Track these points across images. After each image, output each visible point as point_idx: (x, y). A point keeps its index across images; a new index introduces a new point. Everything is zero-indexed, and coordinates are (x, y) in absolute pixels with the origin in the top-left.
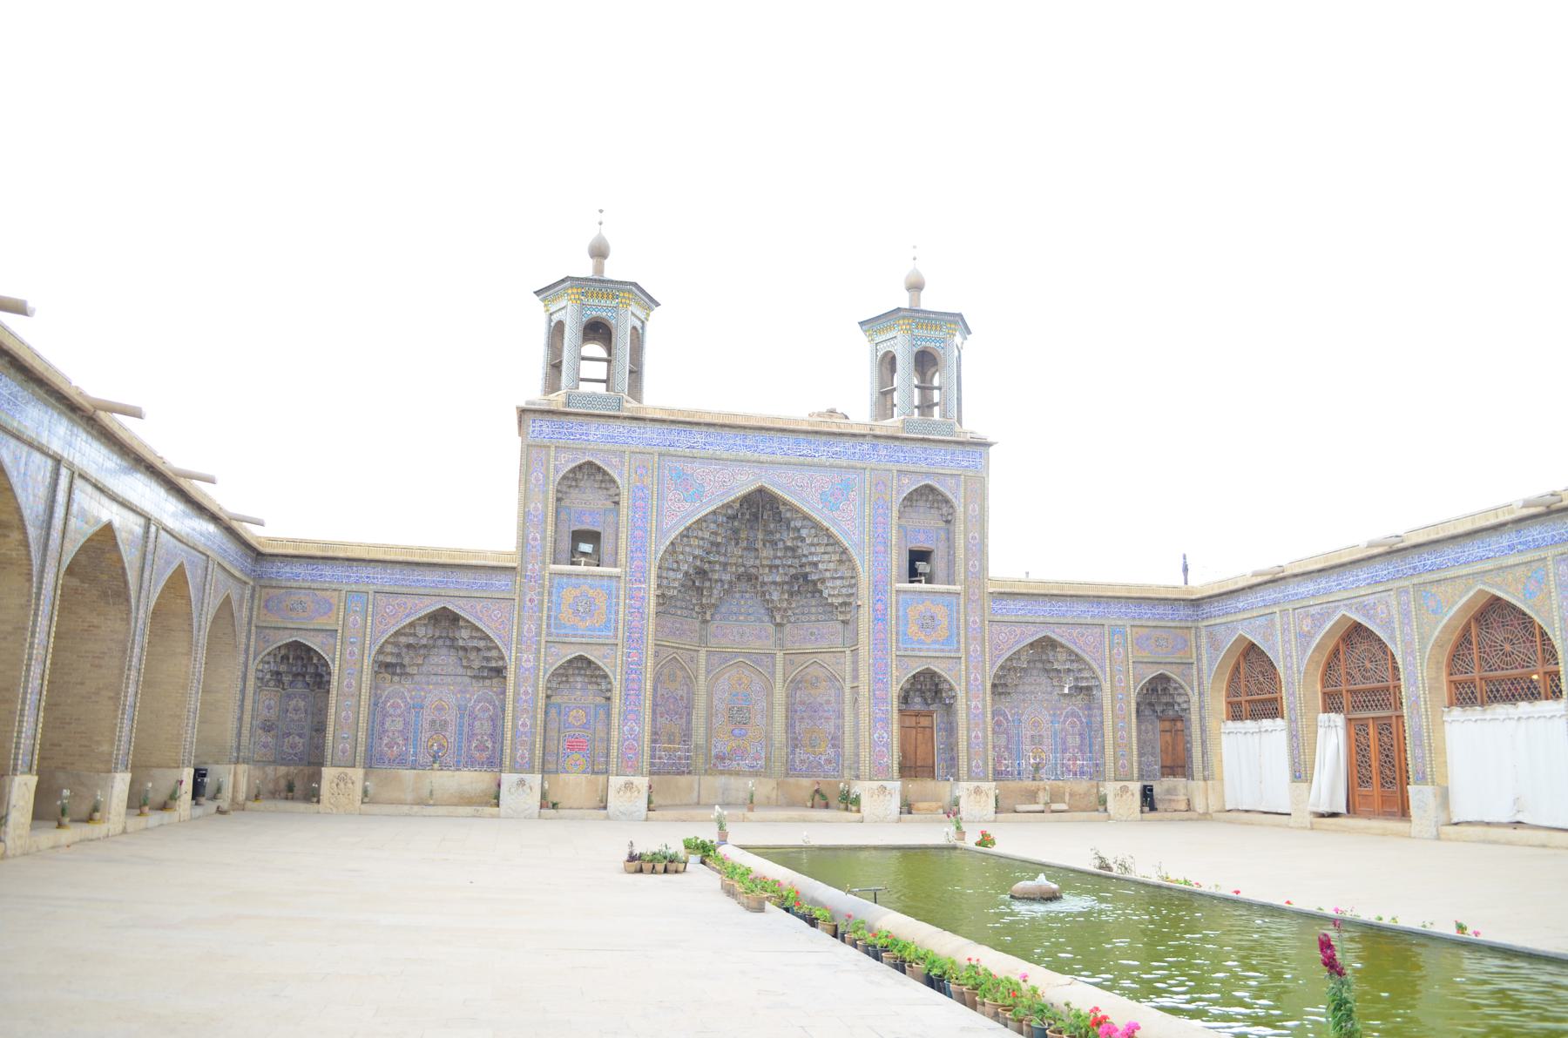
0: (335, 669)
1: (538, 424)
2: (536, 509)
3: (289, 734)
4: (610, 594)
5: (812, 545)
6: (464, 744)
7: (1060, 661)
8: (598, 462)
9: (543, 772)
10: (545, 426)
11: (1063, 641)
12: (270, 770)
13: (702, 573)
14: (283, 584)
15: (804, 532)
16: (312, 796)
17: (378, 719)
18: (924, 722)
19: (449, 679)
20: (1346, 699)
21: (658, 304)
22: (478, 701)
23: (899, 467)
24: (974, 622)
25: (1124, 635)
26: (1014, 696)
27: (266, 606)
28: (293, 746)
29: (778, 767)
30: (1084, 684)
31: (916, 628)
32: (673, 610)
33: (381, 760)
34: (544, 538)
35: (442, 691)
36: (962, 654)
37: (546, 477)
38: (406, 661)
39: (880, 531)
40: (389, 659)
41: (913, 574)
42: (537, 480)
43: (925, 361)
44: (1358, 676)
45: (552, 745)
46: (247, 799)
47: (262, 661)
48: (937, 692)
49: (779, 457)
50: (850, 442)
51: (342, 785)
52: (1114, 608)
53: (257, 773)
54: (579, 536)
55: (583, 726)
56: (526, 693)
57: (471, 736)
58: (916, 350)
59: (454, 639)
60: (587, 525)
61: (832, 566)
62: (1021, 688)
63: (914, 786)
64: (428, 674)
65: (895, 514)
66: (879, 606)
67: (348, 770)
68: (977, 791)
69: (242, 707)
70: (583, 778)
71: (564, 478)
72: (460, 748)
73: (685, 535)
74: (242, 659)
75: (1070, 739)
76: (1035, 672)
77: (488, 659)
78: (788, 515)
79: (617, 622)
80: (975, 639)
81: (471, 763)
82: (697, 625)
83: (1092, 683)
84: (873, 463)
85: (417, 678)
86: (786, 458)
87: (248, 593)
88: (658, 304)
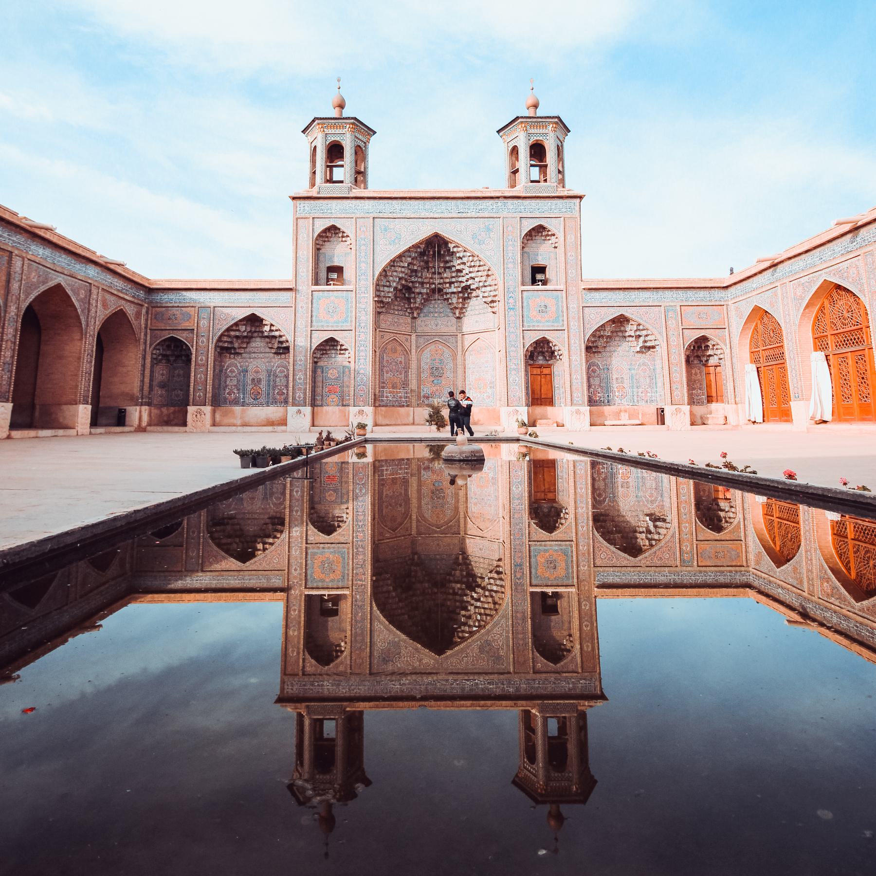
0: (194, 351)
1: (302, 205)
3: (174, 390)
5: (471, 267)
6: (271, 391)
7: (630, 329)
9: (313, 405)
11: (633, 317)
12: (164, 410)
13: (409, 289)
14: (164, 305)
15: (465, 260)
16: (184, 424)
17: (223, 379)
18: (546, 371)
19: (261, 355)
20: (831, 341)
21: (375, 133)
22: (278, 367)
25: (675, 311)
26: (604, 354)
27: (155, 318)
30: (648, 344)
31: (534, 313)
32: (392, 311)
33: (225, 402)
34: (308, 271)
35: (257, 361)
36: (565, 327)
37: (308, 236)
38: (236, 345)
40: (226, 345)
41: (534, 281)
43: (537, 151)
44: (839, 324)
45: (319, 390)
46: (149, 424)
47: (154, 349)
48: (553, 352)
49: (446, 215)
52: (668, 293)
53: (155, 411)
54: (331, 269)
55: (337, 379)
56: (301, 360)
57: (275, 387)
58: (532, 141)
59: (262, 332)
60: (336, 263)
61: (484, 279)
62: (608, 349)
63: (539, 410)
64: (250, 353)
65: (519, 244)
69: (143, 375)
70: (336, 409)
71: (319, 236)
72: (269, 394)
73: (393, 263)
74: (142, 347)
75: (642, 380)
76: (617, 339)
77: (281, 342)
78: (455, 250)
79: (351, 317)
80: (574, 318)
81: (275, 402)
83: (657, 343)
84: (505, 214)
85: (244, 355)
86: (450, 215)
87: (144, 311)
88: (375, 133)
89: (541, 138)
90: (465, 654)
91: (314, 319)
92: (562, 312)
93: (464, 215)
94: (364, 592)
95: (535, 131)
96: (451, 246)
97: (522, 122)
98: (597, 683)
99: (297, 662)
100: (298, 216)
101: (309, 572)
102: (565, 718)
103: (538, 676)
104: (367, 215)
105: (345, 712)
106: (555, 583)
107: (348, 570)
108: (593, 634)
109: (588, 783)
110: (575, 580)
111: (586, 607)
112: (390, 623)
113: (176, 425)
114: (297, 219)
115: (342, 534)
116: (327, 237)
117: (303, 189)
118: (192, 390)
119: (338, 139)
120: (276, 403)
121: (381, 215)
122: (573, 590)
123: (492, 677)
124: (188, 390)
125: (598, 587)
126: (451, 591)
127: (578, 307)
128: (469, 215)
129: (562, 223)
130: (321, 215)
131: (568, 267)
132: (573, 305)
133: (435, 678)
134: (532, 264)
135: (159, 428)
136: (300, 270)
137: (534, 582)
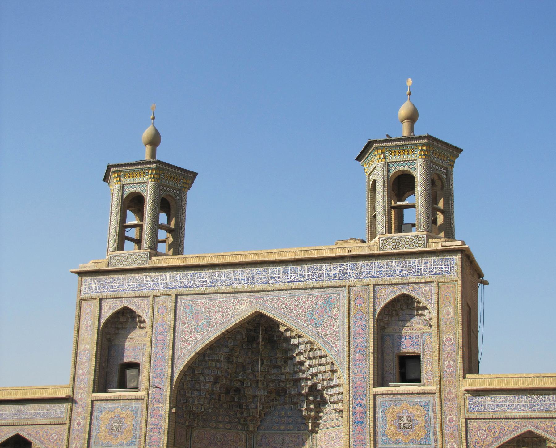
2: (85, 349)
4: (136, 414)
8: (131, 307)
10: (92, 285)
23: (374, 281)
24: (451, 420)
31: (394, 428)
34: (89, 373)
37: (93, 324)
39: (359, 340)
42: (87, 326)
49: (271, 286)
50: (331, 266)
61: (327, 375)
66: (358, 409)
78: (288, 334)
80: (452, 436)
82: (243, 436)
84: (352, 281)
86: (277, 286)
89: (406, 168)
91: (92, 440)
92: (435, 426)
93: (296, 285)
95: (398, 158)
96: (282, 328)
97: (377, 148)
100: (83, 296)
104: (168, 291)
114: (81, 301)
116: (121, 323)
117: (104, 254)
119: (138, 190)
121: (186, 290)
127: (459, 419)
128: (302, 285)
129: (435, 291)
130: (110, 294)
131: (444, 356)
132: (452, 416)
134: (397, 351)
136: (79, 372)
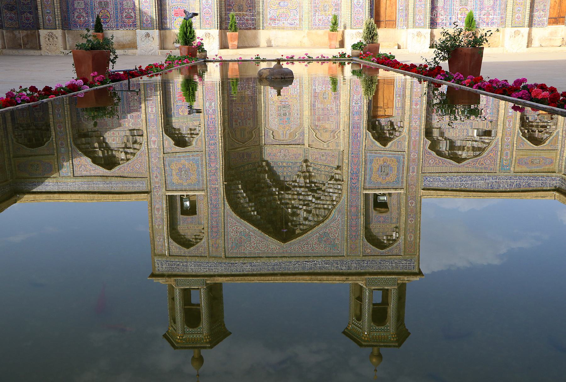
3: (24, 12)
28: (28, 19)
29: (305, 24)
33: (75, 25)
51: (51, 39)
67: (53, 31)
68: (419, 34)
72: (117, 17)
81: (124, 26)
90: (305, 243)
94: (217, 194)
98: (416, 263)
99: (163, 245)
101: (168, 178)
102: (388, 290)
103: (367, 258)
105: (207, 284)
106: (386, 186)
107: (202, 177)
108: (416, 227)
109: (402, 335)
110: (405, 184)
111: (412, 205)
112: (241, 218)
113: (32, 48)
115: (196, 144)
118: (40, 13)
120: (125, 26)
122: (402, 191)
123: (328, 259)
124: (37, 14)
125: (423, 189)
126: (296, 193)
133: (280, 261)
135: (15, 52)
137: (367, 185)
